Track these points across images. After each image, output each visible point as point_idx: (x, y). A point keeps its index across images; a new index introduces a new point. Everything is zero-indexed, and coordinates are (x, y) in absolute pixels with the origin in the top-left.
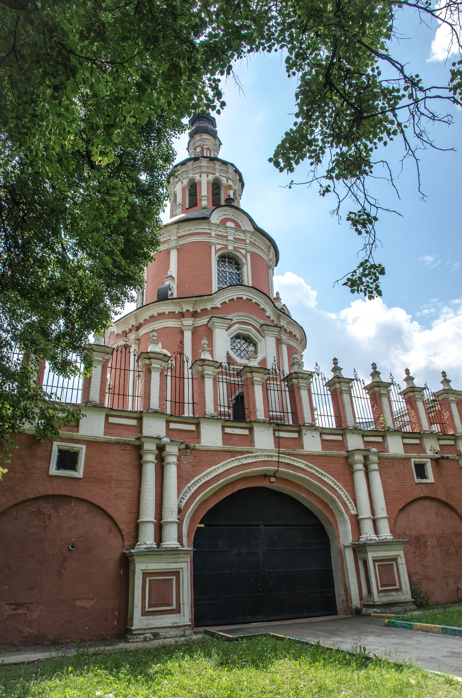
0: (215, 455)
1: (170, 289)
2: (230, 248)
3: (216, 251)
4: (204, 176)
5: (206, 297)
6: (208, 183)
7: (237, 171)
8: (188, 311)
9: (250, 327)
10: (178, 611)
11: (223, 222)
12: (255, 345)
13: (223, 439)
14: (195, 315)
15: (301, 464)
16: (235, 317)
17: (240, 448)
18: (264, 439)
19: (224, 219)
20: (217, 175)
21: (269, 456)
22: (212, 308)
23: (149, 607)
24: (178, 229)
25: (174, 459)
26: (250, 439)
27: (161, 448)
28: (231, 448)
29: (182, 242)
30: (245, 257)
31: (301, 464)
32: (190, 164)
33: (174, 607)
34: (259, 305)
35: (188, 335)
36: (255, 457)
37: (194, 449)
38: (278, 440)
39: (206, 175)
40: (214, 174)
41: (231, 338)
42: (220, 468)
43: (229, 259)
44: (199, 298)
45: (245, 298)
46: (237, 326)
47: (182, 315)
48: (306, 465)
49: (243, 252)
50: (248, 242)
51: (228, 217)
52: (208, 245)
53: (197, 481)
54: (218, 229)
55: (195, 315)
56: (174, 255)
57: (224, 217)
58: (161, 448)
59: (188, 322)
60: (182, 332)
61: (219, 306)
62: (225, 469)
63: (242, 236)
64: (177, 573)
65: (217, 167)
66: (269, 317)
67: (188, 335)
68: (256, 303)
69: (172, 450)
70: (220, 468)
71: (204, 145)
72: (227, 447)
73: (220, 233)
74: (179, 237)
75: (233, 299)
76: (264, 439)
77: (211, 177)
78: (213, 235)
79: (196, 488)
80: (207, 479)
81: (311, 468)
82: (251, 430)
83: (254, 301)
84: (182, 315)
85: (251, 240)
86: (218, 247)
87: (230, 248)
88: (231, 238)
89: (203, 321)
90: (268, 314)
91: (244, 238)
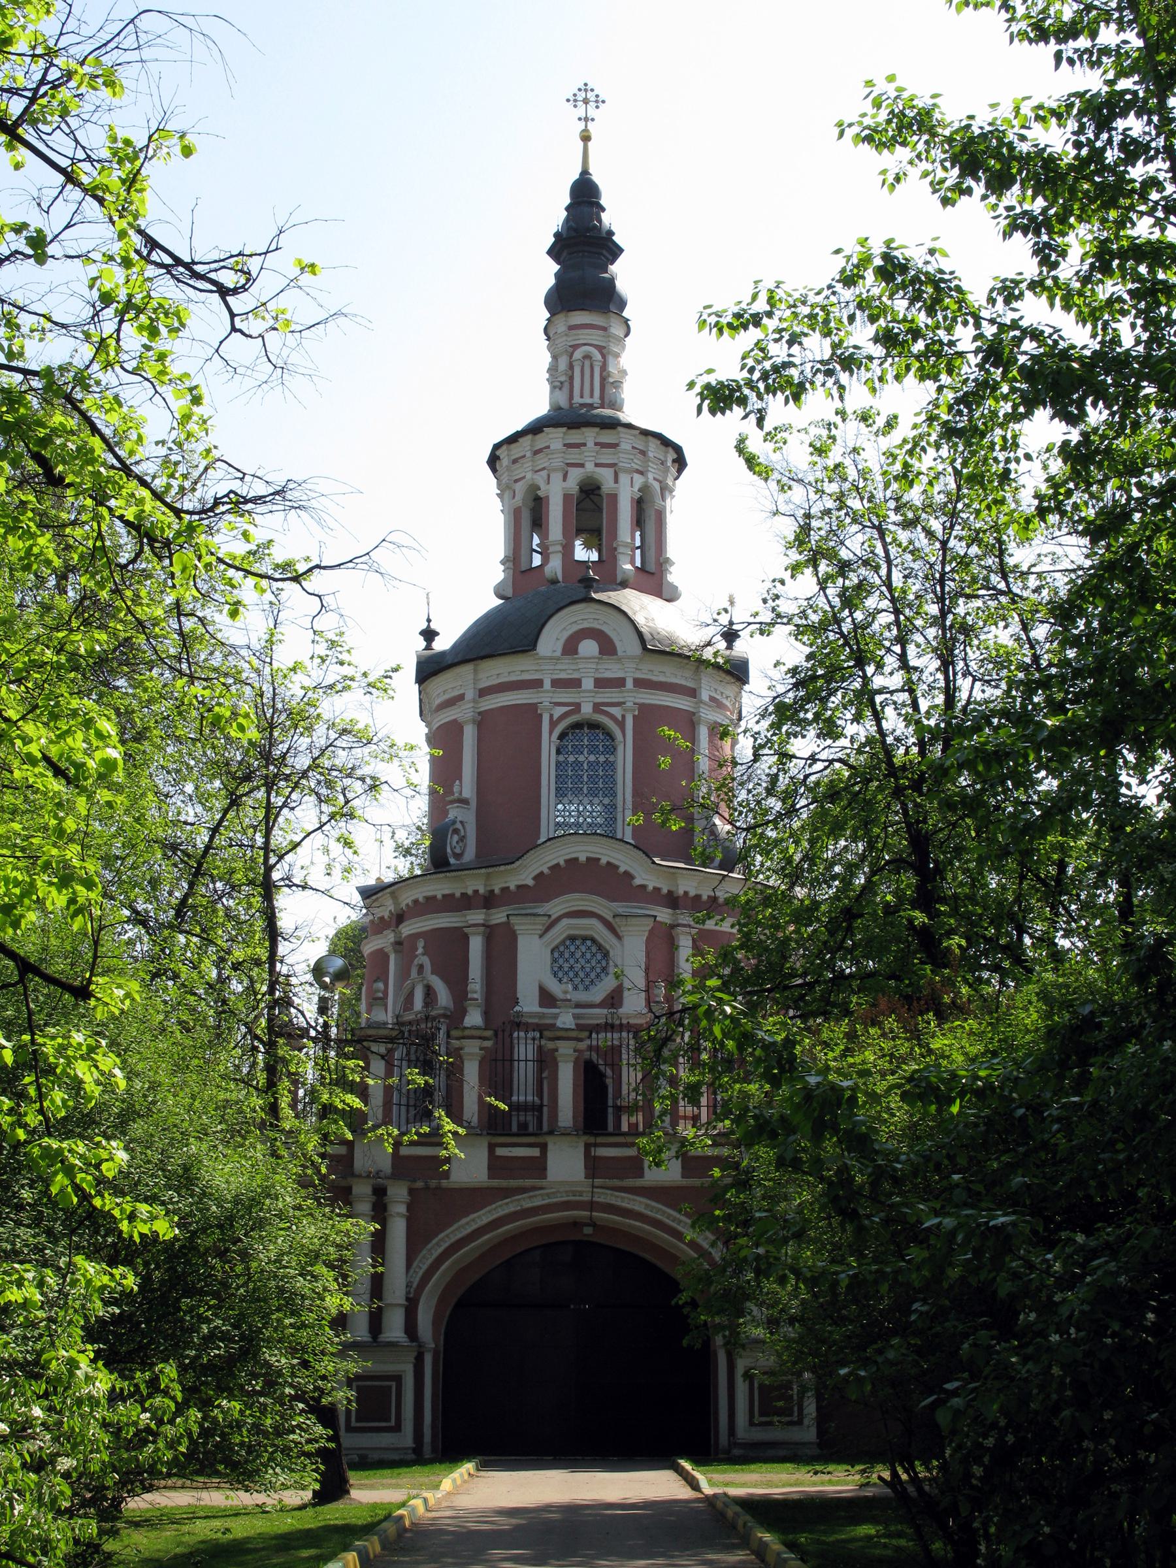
0: (475, 1197)
1: (456, 831)
2: (587, 709)
3: (553, 724)
4: (557, 477)
5: (502, 868)
6: (567, 497)
7: (646, 433)
8: (476, 892)
9: (594, 922)
10: (397, 1428)
11: (570, 648)
13: (490, 1168)
14: (489, 901)
15: (639, 1204)
16: (556, 907)
17: (528, 1182)
18: (566, 1164)
19: (576, 633)
21: (574, 1193)
22: (519, 887)
23: (357, 1420)
24: (476, 671)
25: (402, 1209)
26: (538, 1167)
27: (380, 1192)
28: (503, 1183)
30: (621, 724)
31: (639, 1204)
32: (526, 441)
33: (393, 1423)
34: (617, 867)
35: (476, 945)
36: (548, 1195)
37: (438, 1188)
38: (594, 1167)
39: (560, 475)
40: (582, 465)
41: (552, 951)
42: (483, 1217)
43: (585, 731)
44: (490, 870)
45: (582, 858)
46: (565, 921)
47: (465, 902)
48: (647, 1206)
49: (616, 711)
50: (629, 684)
51: (586, 625)
53: (442, 1240)
54: (559, 667)
55: (489, 901)
56: (469, 735)
57: (576, 628)
58: (380, 1192)
59: (477, 916)
60: (465, 938)
61: (531, 883)
62: (491, 1218)
63: (612, 671)
64: (398, 1379)
65: (590, 444)
66: (644, 887)
67: (476, 945)
68: (608, 863)
69: (398, 1194)
70: (483, 1217)
71: (575, 347)
72: (496, 1183)
73: (563, 676)
74: (483, 693)
75: (558, 865)
76: (566, 1164)
77: (572, 484)
78: (547, 684)
79: (440, 1250)
80: (459, 1236)
81: (658, 1210)
82: (544, 1147)
83: (604, 861)
84: (465, 902)
85: (639, 675)
86: (559, 711)
87: (587, 709)
88: (588, 684)
89: (498, 916)
90: (638, 881)
91: (620, 675)
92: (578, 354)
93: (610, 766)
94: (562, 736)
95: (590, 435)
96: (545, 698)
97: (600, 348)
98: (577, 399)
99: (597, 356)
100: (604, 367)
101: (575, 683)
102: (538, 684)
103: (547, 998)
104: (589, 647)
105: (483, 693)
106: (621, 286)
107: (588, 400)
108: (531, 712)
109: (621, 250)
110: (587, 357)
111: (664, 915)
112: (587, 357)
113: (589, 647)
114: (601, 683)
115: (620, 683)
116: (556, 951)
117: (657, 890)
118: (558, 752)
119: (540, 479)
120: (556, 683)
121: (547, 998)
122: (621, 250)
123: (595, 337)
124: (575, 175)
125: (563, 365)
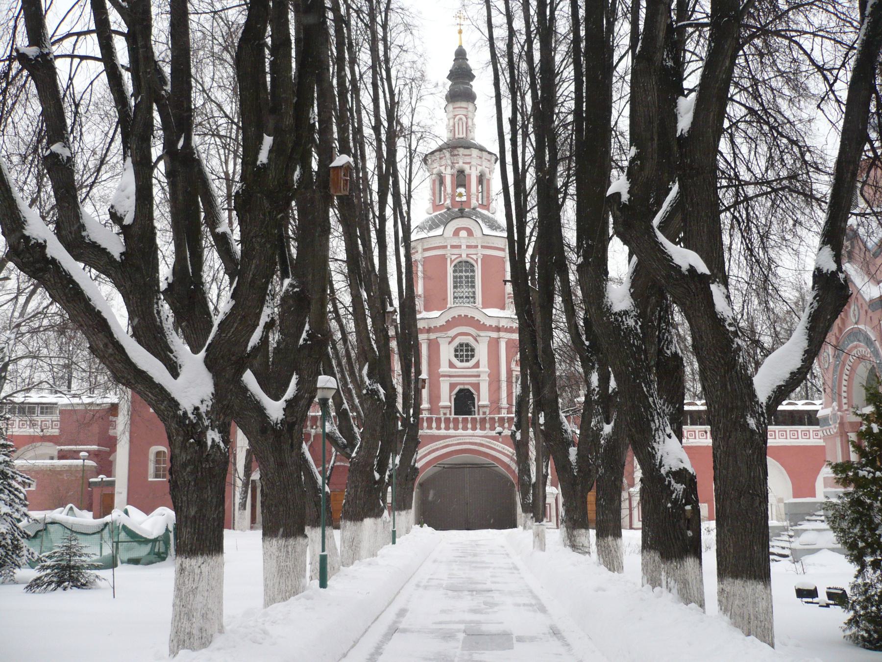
2: (464, 257)
3: (452, 261)
4: (449, 168)
9: (470, 338)
11: (456, 233)
12: (473, 350)
20: (461, 164)
29: (428, 254)
30: (476, 261)
43: (465, 266)
49: (474, 257)
52: (443, 258)
71: (456, 116)
78: (449, 247)
86: (453, 257)
88: (464, 247)
89: (433, 336)
92: (457, 118)
93: (473, 277)
94: (455, 266)
95: (461, 151)
96: (448, 252)
97: (465, 116)
98: (457, 136)
99: (464, 119)
100: (467, 123)
101: (459, 247)
102: (445, 247)
103: (451, 365)
104: (463, 234)
105: (425, 250)
106: (474, 89)
107: (461, 136)
108: (443, 258)
109: (474, 77)
110: (461, 119)
111: (494, 335)
112: (461, 119)
113: (463, 234)
114: (468, 247)
115: (476, 247)
116: (456, 351)
117: (490, 326)
118: (455, 271)
119: (442, 168)
120: (453, 247)
121: (451, 365)
122: (474, 77)
123: (464, 112)
124: (456, 47)
125: (451, 124)
